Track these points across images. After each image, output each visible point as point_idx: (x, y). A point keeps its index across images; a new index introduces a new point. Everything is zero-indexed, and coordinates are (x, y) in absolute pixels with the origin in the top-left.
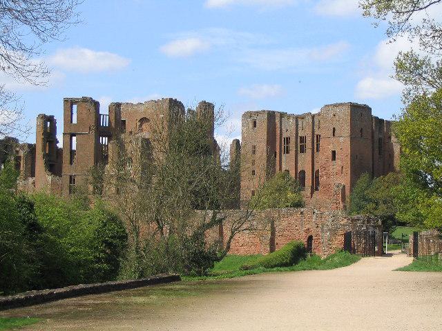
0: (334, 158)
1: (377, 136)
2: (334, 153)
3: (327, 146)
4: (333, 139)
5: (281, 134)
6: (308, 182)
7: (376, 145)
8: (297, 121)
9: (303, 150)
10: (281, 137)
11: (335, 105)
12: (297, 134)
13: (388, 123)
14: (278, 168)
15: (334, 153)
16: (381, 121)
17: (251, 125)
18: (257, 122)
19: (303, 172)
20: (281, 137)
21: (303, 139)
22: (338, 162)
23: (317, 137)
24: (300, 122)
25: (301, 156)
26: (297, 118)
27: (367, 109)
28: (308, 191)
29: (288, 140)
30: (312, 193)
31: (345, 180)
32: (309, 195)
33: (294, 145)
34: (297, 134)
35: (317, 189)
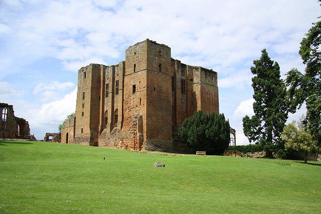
0: (134, 91)
1: (179, 76)
2: (134, 86)
4: (133, 75)
7: (179, 85)
10: (104, 85)
11: (138, 43)
12: (114, 78)
13: (190, 67)
15: (134, 86)
16: (184, 66)
22: (137, 94)
24: (116, 70)
26: (114, 67)
27: (166, 49)
28: (119, 125)
31: (143, 111)
34: (114, 78)
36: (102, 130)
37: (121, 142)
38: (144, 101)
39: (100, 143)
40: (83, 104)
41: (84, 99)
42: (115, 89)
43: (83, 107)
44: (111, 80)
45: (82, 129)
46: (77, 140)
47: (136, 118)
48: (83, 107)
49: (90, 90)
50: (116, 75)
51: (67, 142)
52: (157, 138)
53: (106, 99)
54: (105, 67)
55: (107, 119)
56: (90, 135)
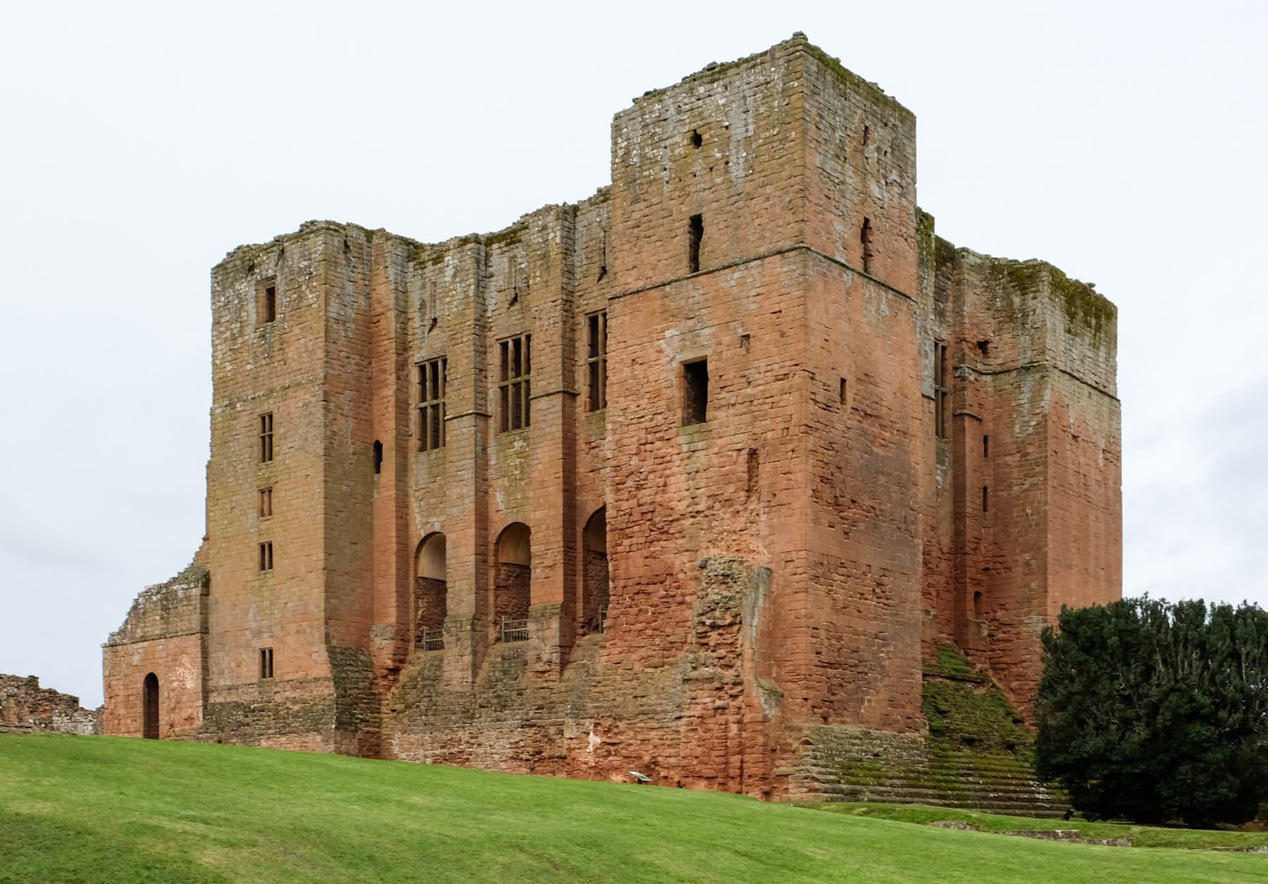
2: (696, 373)
3: (646, 358)
5: (403, 347)
6: (547, 587)
8: (483, 261)
9: (517, 413)
10: (402, 366)
12: (482, 325)
14: (412, 573)
15: (696, 373)
17: (252, 312)
18: (280, 288)
19: (518, 533)
20: (402, 366)
21: (517, 355)
23: (593, 321)
25: (505, 453)
26: (480, 247)
28: (543, 638)
29: (434, 373)
30: (566, 647)
31: (776, 538)
32: (549, 651)
33: (468, 393)
34: (482, 325)
35: (593, 625)
36: (401, 658)
37: (594, 740)
38: (795, 473)
39: (396, 742)
40: (267, 492)
41: (267, 453)
42: (493, 393)
43: (265, 512)
44: (467, 336)
45: (267, 658)
46: (225, 721)
47: (726, 578)
48: (265, 512)
49: (311, 397)
50: (495, 300)
51: (151, 729)
52: (858, 719)
53: (420, 465)
54: (412, 249)
55: (438, 588)
56: (328, 691)
